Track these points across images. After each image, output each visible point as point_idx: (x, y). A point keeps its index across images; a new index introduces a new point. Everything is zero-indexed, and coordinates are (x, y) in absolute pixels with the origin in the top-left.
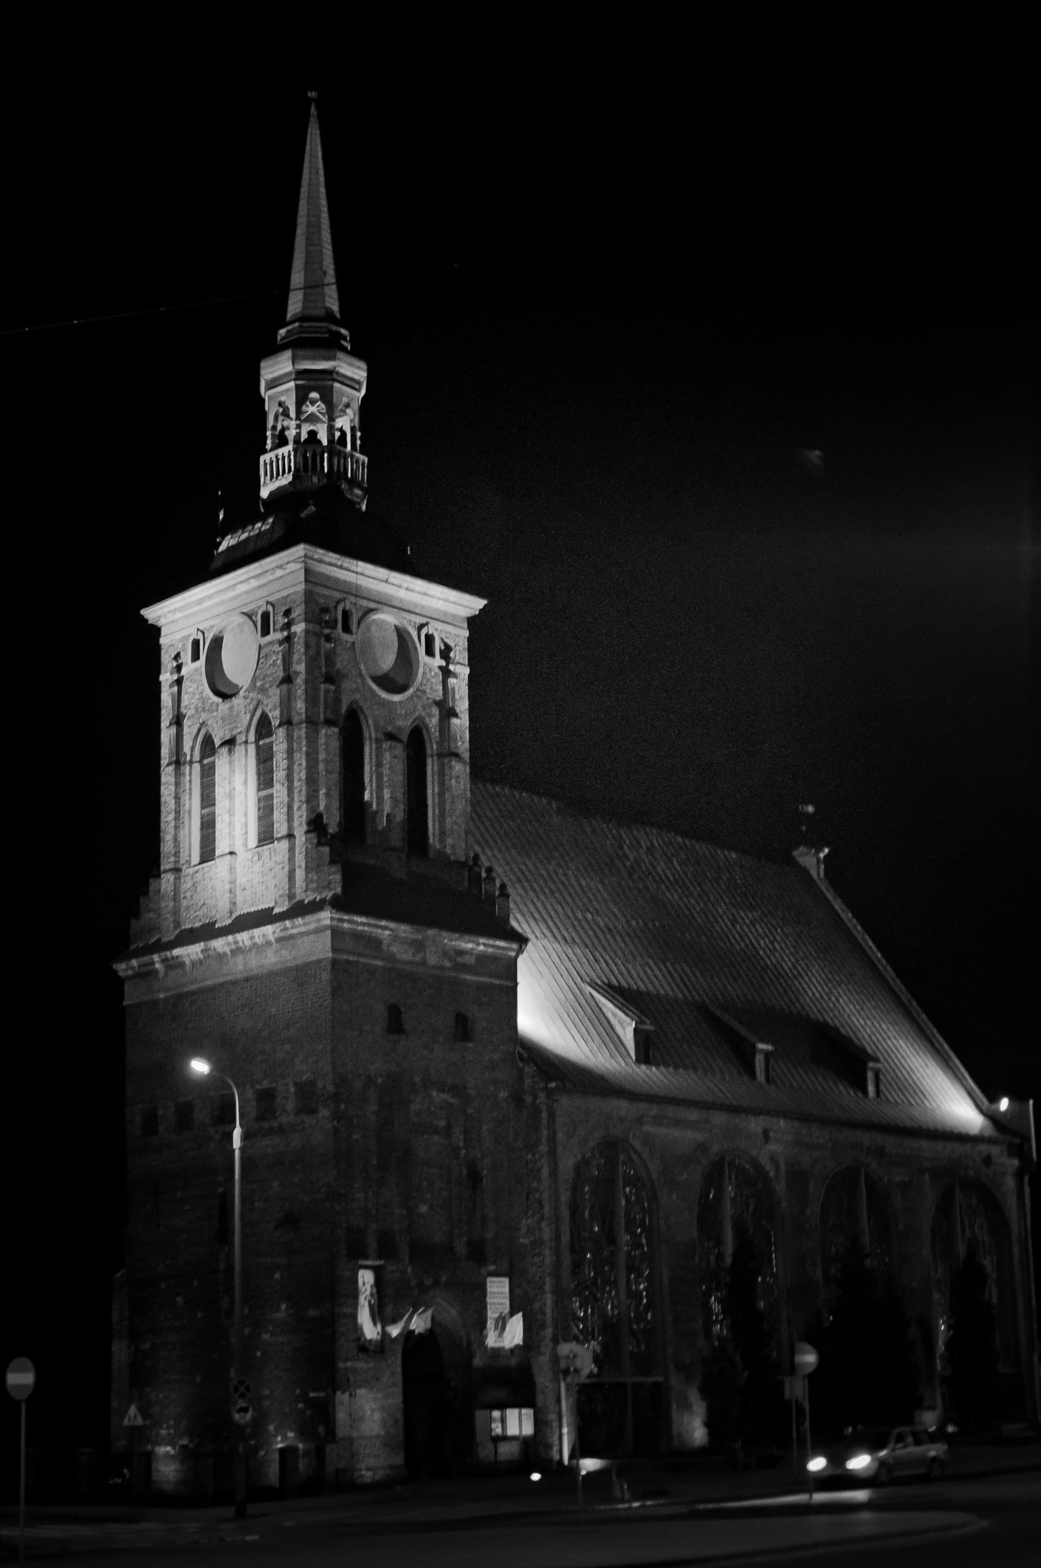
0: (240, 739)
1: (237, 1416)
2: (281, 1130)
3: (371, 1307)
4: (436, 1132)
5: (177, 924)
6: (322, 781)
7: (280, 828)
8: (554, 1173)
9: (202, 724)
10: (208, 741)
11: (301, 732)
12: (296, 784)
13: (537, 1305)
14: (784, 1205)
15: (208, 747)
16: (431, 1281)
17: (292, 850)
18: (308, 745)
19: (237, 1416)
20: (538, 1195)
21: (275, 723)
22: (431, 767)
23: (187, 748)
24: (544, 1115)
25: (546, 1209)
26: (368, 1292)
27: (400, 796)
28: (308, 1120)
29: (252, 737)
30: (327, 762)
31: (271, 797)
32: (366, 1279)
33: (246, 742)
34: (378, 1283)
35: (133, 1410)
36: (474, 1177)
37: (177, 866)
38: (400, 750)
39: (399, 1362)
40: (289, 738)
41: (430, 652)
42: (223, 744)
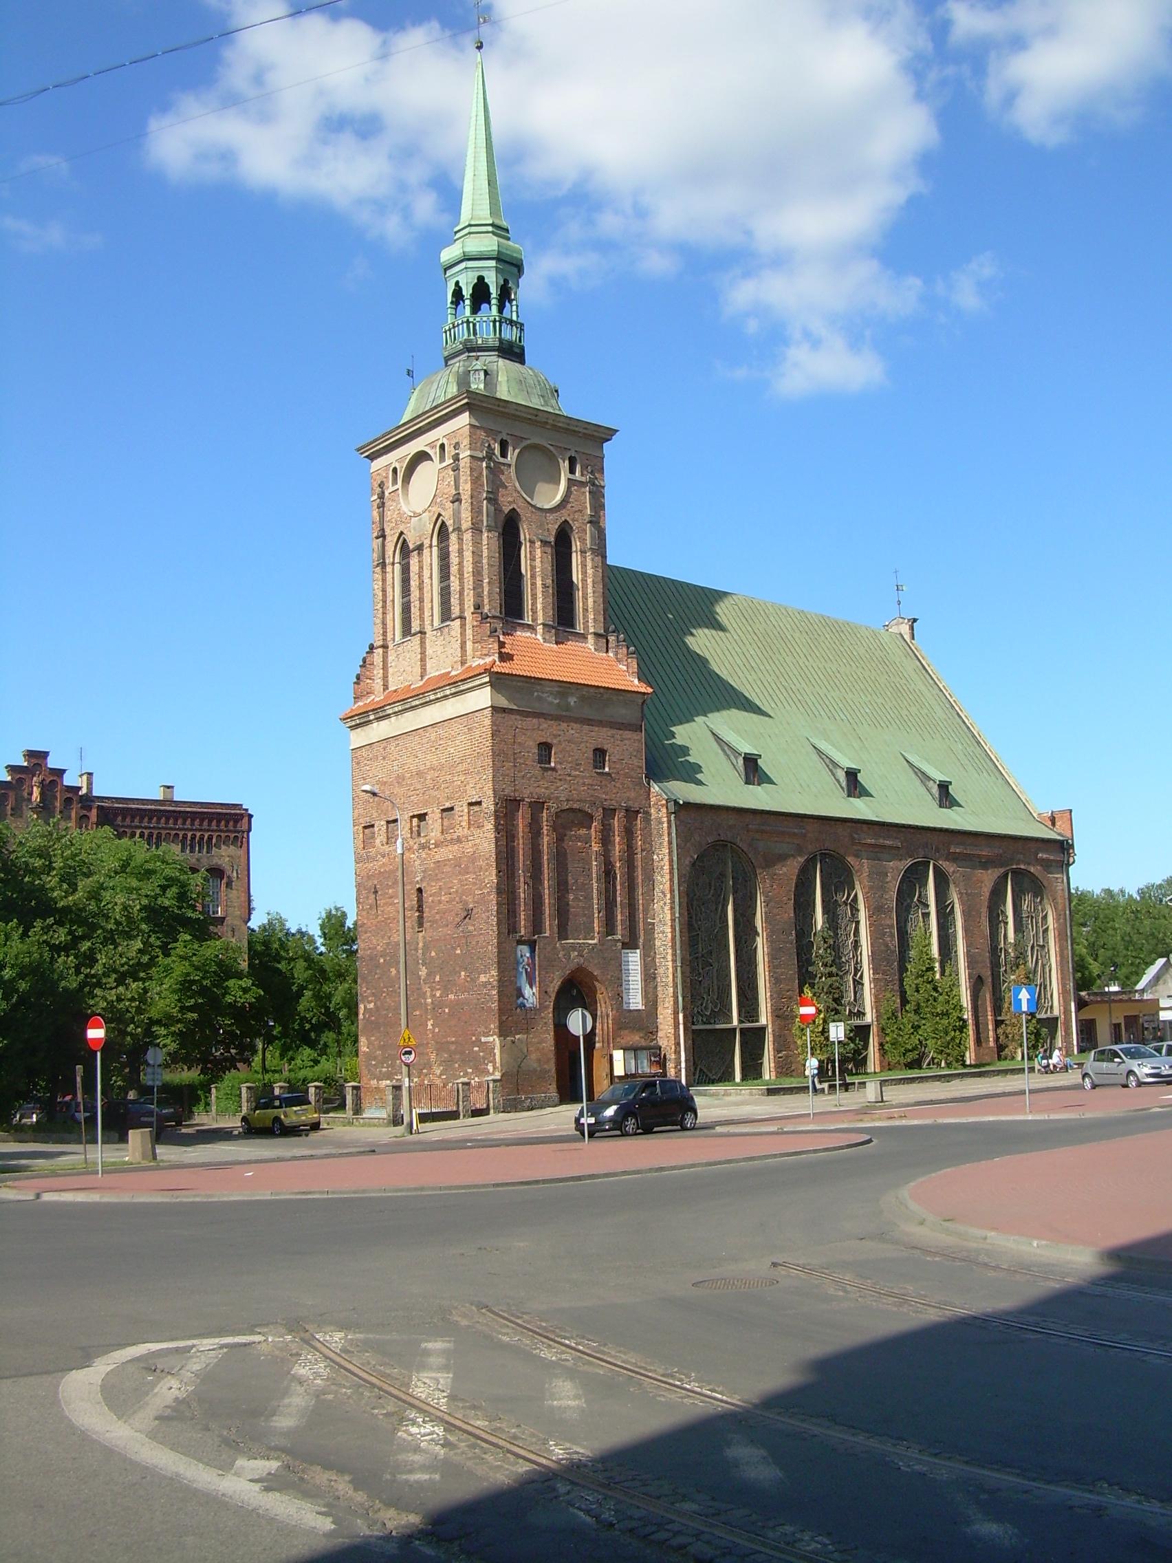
0: (427, 543)
2: (459, 840)
5: (386, 687)
6: (485, 572)
7: (455, 611)
9: (402, 533)
11: (467, 536)
12: (466, 575)
15: (405, 551)
17: (463, 626)
18: (473, 545)
21: (451, 529)
23: (389, 552)
24: (665, 825)
27: (549, 582)
28: (476, 832)
29: (435, 542)
30: (489, 557)
33: (431, 546)
40: (460, 540)
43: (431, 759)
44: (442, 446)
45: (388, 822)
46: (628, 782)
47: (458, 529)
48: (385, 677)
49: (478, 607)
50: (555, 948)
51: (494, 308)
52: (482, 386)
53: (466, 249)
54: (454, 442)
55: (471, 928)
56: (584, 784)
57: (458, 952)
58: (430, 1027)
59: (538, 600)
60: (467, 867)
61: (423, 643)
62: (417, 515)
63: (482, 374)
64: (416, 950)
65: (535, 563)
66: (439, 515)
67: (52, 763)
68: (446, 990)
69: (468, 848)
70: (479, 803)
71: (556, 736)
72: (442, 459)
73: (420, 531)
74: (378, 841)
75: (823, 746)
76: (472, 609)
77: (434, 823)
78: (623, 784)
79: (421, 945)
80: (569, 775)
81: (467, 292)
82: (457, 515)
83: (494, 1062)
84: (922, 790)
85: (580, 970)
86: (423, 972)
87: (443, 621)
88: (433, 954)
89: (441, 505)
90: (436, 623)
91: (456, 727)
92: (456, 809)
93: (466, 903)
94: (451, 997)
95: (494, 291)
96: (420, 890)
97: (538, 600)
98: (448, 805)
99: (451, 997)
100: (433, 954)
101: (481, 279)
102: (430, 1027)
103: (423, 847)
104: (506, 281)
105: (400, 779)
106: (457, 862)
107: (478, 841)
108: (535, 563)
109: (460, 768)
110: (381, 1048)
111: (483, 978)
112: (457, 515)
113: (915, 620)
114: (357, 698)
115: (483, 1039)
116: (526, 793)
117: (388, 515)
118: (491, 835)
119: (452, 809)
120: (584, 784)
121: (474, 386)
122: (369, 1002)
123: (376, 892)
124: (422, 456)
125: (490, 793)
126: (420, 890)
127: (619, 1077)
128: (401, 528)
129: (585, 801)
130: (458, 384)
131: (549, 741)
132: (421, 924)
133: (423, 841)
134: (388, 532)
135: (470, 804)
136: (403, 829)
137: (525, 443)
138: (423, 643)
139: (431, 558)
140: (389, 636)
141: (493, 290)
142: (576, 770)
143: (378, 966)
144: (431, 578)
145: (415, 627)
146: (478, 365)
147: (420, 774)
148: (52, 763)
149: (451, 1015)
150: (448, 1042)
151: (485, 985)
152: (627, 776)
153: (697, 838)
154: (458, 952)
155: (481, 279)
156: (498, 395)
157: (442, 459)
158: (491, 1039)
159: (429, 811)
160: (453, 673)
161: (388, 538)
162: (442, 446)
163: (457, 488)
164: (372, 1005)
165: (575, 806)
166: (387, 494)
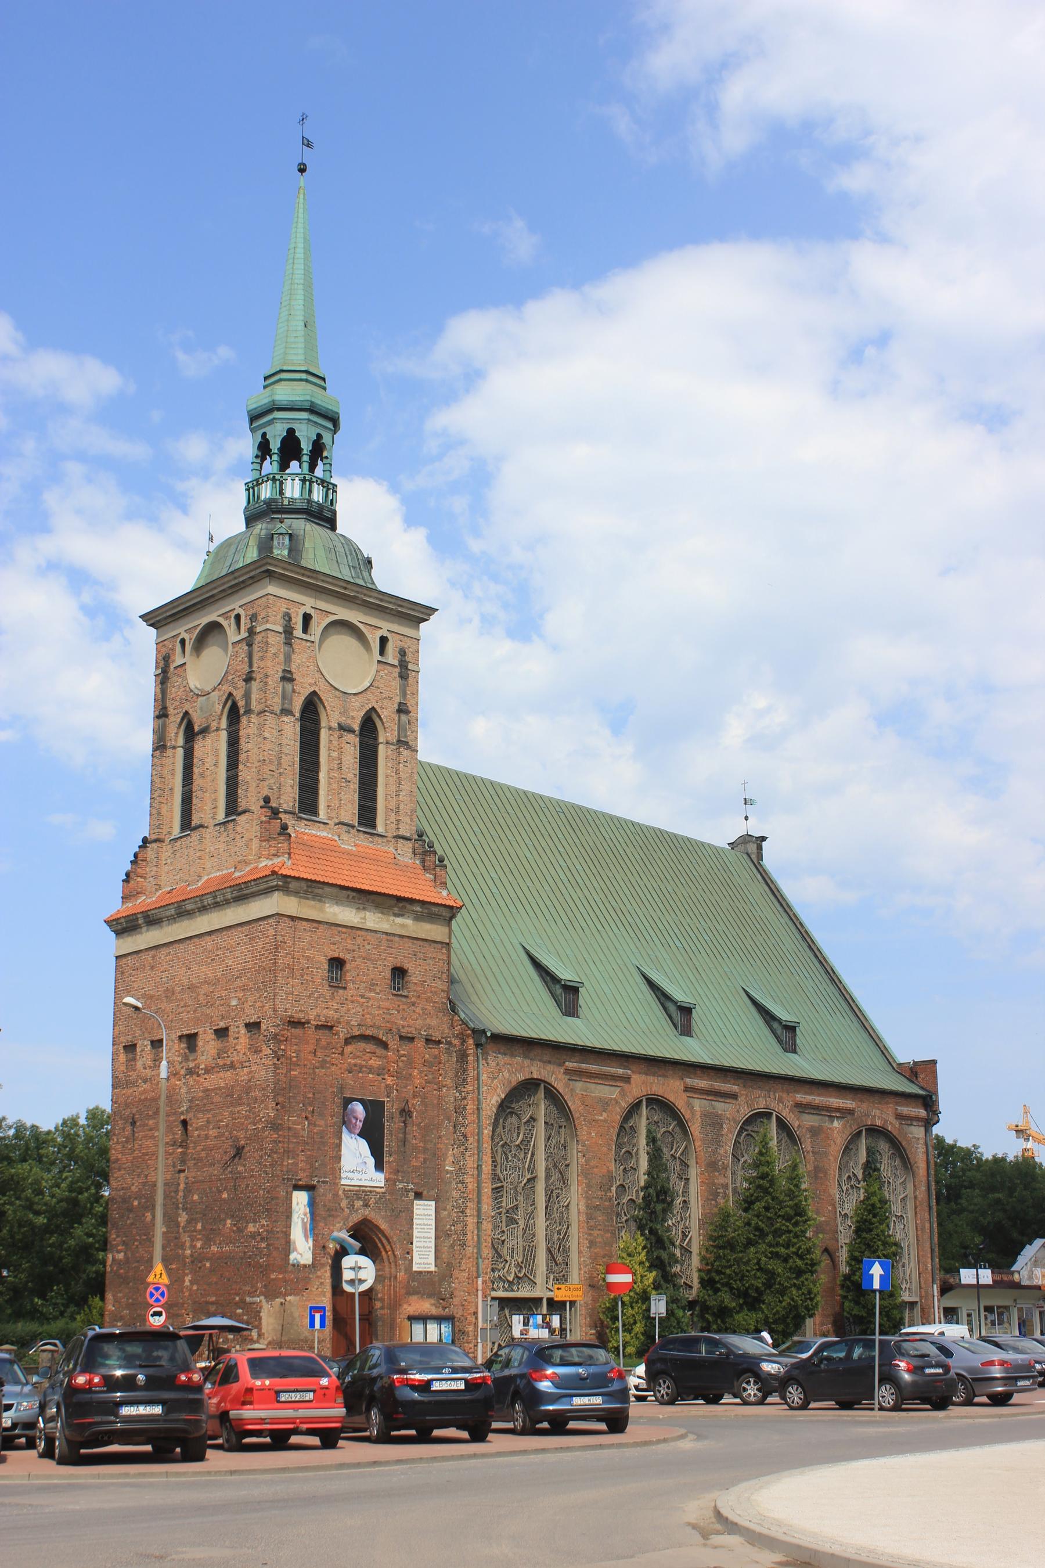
0: (214, 725)
1: (151, 1319)
2: (232, 1066)
3: (304, 1224)
7: (242, 804)
10: (190, 727)
14: (698, 1144)
15: (191, 734)
16: (361, 1203)
19: (151, 1319)
20: (463, 1129)
21: (242, 711)
22: (383, 752)
25: (471, 1140)
26: (302, 1211)
28: (254, 1057)
29: (224, 724)
31: (237, 776)
34: (312, 1204)
37: (162, 836)
39: (328, 1274)
41: (382, 652)
43: (207, 971)
44: (238, 617)
45: (152, 1042)
46: (429, 1007)
47: (248, 711)
49: (267, 800)
50: (336, 1195)
51: (306, 466)
52: (286, 552)
53: (277, 398)
54: (250, 613)
55: (240, 1168)
56: (379, 1007)
57: (225, 1195)
58: (187, 1283)
59: (338, 795)
60: (240, 1098)
61: (201, 839)
63: (287, 537)
64: (177, 1191)
65: (338, 756)
66: (230, 694)
68: (208, 1241)
69: (243, 1075)
71: (349, 951)
73: (210, 711)
74: (139, 1064)
76: (263, 803)
77: (208, 1046)
78: (423, 1009)
79: (182, 1186)
80: (363, 996)
81: (275, 445)
83: (259, 1327)
84: (766, 1031)
86: (183, 1218)
87: (227, 815)
88: (196, 1197)
89: (233, 683)
90: (221, 816)
91: (238, 935)
92: (232, 1030)
93: (237, 1139)
94: (214, 1248)
95: (306, 446)
96: (185, 1123)
97: (338, 795)
98: (222, 1025)
99: (214, 1248)
100: (196, 1197)
101: (291, 432)
102: (187, 1283)
103: (191, 1072)
104: (319, 436)
106: (228, 1092)
107: (253, 1068)
108: (338, 756)
109: (239, 983)
110: (128, 1306)
111: (251, 1228)
112: (247, 695)
113: (763, 839)
114: (125, 898)
115: (248, 1299)
116: (312, 1015)
119: (227, 1029)
120: (379, 1007)
121: (276, 552)
122: (119, 1252)
124: (214, 627)
125: (270, 1012)
128: (187, 707)
129: (379, 1027)
130: (260, 550)
131: (342, 956)
133: (191, 1065)
134: (171, 711)
141: (306, 446)
142: (371, 990)
143: (130, 1210)
145: (195, 821)
146: (282, 528)
147: (192, 988)
149: (212, 1270)
150: (207, 1303)
151: (253, 1236)
152: (429, 1000)
153: (506, 1074)
154: (225, 1195)
155: (291, 432)
156: (303, 563)
158: (258, 1300)
159: (201, 1030)
160: (237, 874)
161: (172, 719)
163: (251, 665)
164: (121, 1256)
165: (369, 1032)
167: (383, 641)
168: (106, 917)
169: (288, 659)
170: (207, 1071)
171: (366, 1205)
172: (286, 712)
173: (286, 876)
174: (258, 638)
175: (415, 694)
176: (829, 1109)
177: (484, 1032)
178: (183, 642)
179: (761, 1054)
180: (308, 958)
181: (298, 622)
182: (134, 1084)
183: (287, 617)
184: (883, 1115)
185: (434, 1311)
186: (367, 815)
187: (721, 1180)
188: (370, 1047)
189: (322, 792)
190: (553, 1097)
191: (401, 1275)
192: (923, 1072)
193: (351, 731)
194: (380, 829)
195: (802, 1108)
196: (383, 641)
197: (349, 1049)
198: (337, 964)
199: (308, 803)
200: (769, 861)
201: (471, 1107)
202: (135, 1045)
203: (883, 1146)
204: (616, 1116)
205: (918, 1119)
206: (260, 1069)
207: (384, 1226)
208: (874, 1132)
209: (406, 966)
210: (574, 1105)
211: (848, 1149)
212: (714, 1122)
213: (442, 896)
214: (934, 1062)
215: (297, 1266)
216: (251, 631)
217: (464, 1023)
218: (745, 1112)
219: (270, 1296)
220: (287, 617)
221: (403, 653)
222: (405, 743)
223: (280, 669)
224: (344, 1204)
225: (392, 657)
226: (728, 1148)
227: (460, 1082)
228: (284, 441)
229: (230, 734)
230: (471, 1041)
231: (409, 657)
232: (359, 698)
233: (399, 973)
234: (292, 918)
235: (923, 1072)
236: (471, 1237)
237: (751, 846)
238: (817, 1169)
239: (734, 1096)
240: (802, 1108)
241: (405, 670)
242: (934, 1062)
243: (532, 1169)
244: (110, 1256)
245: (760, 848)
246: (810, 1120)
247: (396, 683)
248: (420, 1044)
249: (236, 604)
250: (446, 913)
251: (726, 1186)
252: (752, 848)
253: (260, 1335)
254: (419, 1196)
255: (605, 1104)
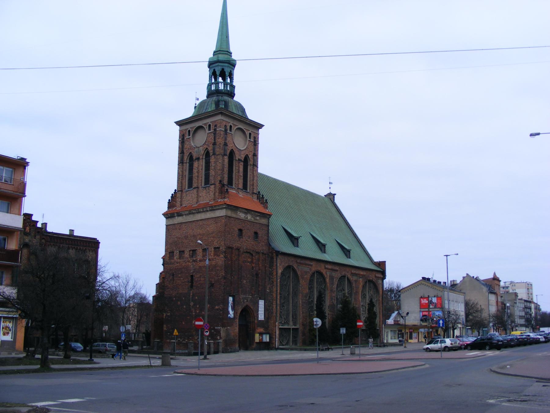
0: (201, 157)
4: (248, 262)
5: (181, 205)
8: (277, 274)
13: (271, 308)
17: (215, 187)
28: (217, 258)
29: (204, 157)
32: (231, 299)
33: (202, 159)
34: (234, 300)
35: (176, 331)
36: (257, 275)
38: (242, 163)
41: (250, 138)
42: (196, 159)
44: (210, 125)
47: (214, 154)
48: (181, 202)
49: (220, 181)
62: (197, 147)
64: (189, 296)
65: (239, 168)
67: (34, 218)
70: (218, 248)
72: (209, 129)
74: (175, 258)
75: (314, 235)
82: (214, 150)
83: (220, 336)
84: (342, 252)
85: (247, 306)
86: (192, 304)
87: (205, 184)
89: (208, 145)
90: (203, 185)
96: (192, 276)
103: (194, 261)
105: (186, 237)
111: (217, 307)
113: (335, 194)
117: (185, 146)
118: (223, 259)
121: (221, 106)
123: (173, 275)
124: (200, 127)
125: (223, 245)
126: (192, 276)
127: (257, 343)
128: (191, 151)
130: (216, 105)
132: (192, 286)
134: (185, 151)
135: (215, 248)
136: (187, 254)
137: (237, 127)
138: (197, 191)
139: (203, 163)
140: (184, 188)
141: (227, 74)
144: (202, 169)
145: (195, 185)
148: (34, 218)
151: (217, 309)
152: (263, 242)
157: (209, 129)
162: (210, 125)
163: (215, 140)
166: (185, 138)
167: (250, 134)
168: (163, 212)
169: (226, 139)
170: (200, 261)
171: (247, 301)
172: (225, 155)
173: (228, 205)
174: (217, 132)
175: (258, 150)
176: (359, 274)
177: (279, 252)
178: (189, 131)
179: (341, 259)
180: (233, 229)
181: (229, 127)
182: (173, 264)
183: (226, 126)
184: (372, 277)
185: (264, 331)
186: (245, 187)
187: (334, 295)
188: (248, 255)
189: (234, 179)
190: (294, 271)
191: (256, 321)
192: (382, 265)
193: (242, 161)
194: (248, 191)
195: (353, 274)
196: (250, 134)
197: (243, 256)
198: (240, 230)
199: (230, 182)
200: (336, 201)
201: (275, 273)
202: (173, 252)
203: (372, 285)
204: (308, 276)
205: (380, 278)
206: (220, 260)
207: (252, 307)
208: (371, 281)
209: (258, 232)
210: (299, 273)
211: (364, 287)
212: (332, 278)
213: (266, 211)
214: (385, 262)
215: (230, 318)
216: (215, 130)
217: (273, 249)
218: (340, 276)
219: (223, 326)
220: (226, 126)
221: (255, 138)
222: (255, 165)
223: (223, 142)
224: (242, 300)
225: (252, 140)
226: (335, 286)
227: (271, 266)
228: (221, 72)
229: (206, 160)
230: (275, 254)
231: (256, 139)
232: (244, 152)
233: (256, 233)
234: (229, 217)
235: (382, 265)
236: (274, 311)
237: (331, 197)
238: (356, 292)
239: (337, 271)
240: (353, 274)
241: (255, 143)
242: (385, 262)
243: (289, 291)
244: (165, 314)
245: (334, 197)
246: (355, 278)
247: (252, 147)
248: (261, 255)
249: (209, 121)
250: (268, 217)
251: (334, 297)
252: (332, 197)
253: (221, 338)
254: (260, 299)
255: (306, 273)
